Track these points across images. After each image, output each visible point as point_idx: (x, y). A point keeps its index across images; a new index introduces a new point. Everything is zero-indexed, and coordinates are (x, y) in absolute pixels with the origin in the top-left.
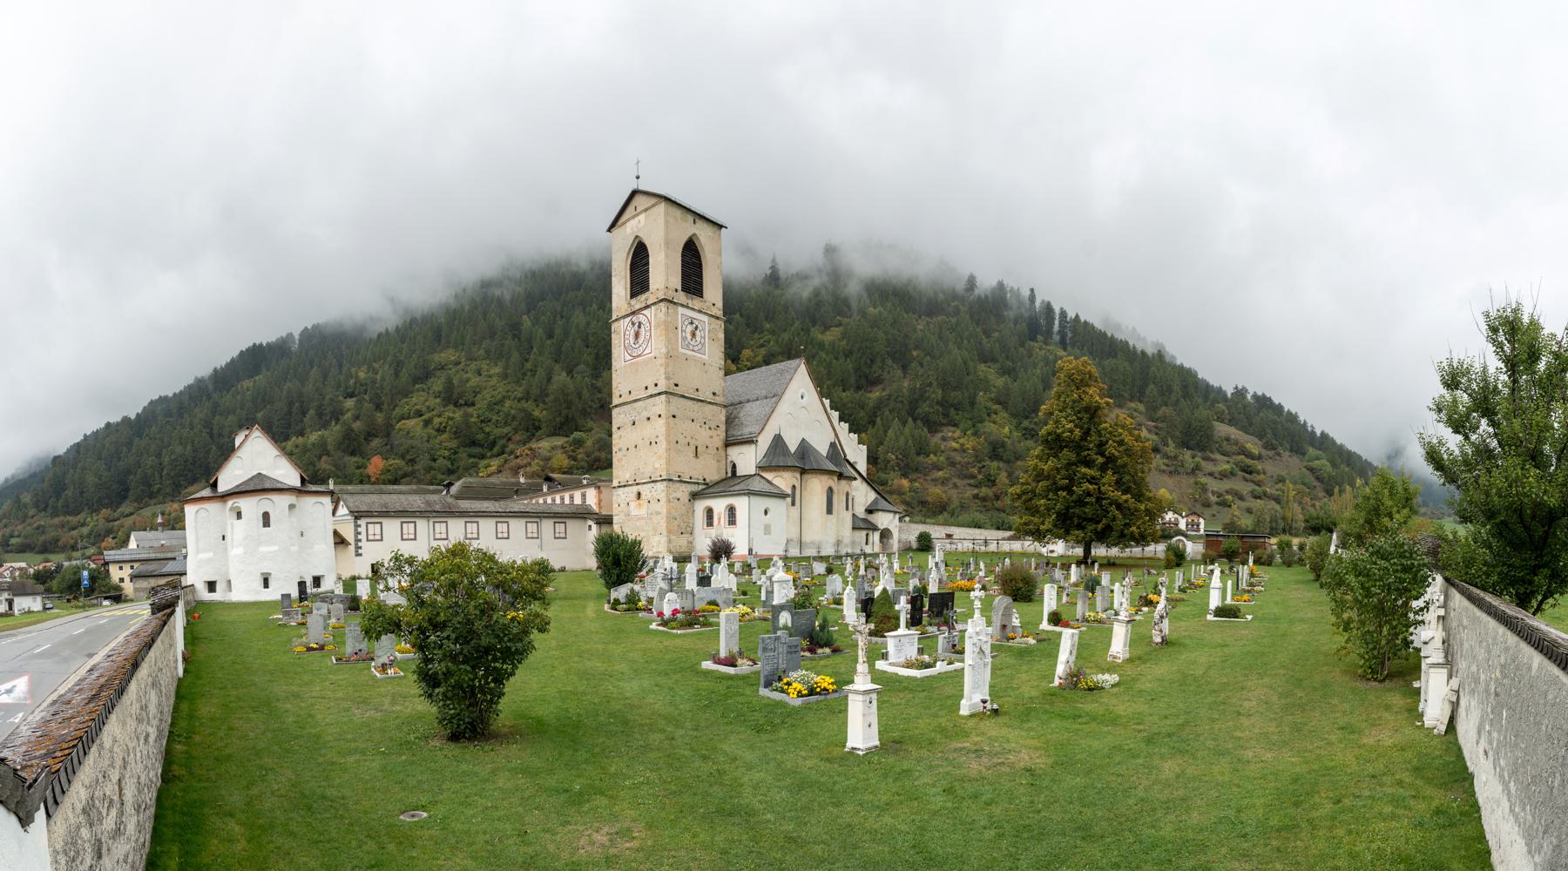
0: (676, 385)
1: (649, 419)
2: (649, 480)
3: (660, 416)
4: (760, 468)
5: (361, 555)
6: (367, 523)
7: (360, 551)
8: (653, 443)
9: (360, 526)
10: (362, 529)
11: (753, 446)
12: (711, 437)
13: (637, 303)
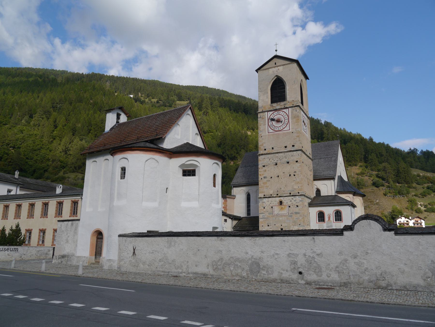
1: (288, 163)
2: (289, 195)
3: (297, 162)
4: (337, 192)
8: (292, 175)
11: (332, 181)
13: (276, 106)
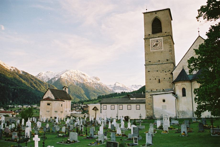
0: (150, 62)
5: (101, 113)
6: (103, 105)
7: (101, 112)
9: (102, 106)
10: (102, 107)
12: (166, 75)
